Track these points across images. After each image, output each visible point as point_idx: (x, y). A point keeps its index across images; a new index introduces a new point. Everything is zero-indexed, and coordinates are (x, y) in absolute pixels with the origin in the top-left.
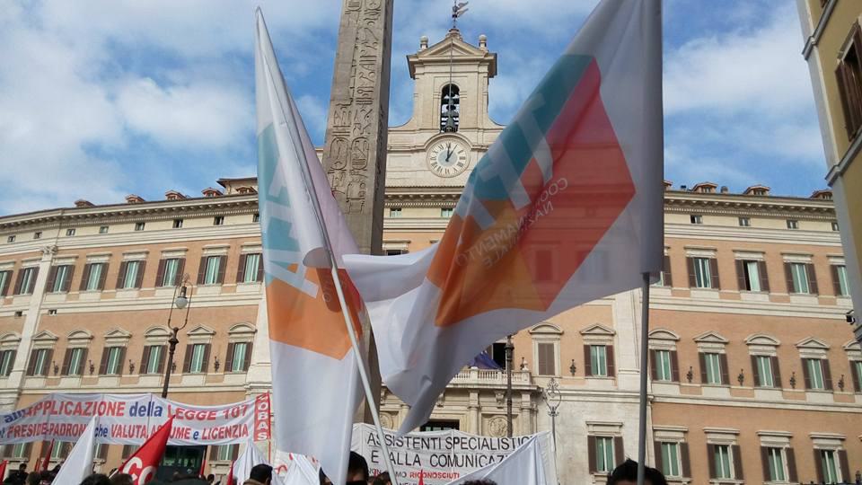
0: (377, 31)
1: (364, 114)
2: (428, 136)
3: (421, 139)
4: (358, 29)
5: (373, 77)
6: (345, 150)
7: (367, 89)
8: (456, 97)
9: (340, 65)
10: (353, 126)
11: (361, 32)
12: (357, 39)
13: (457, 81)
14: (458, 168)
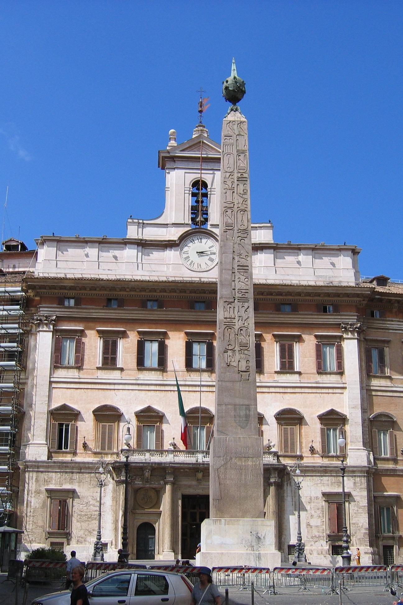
0: (247, 246)
1: (244, 309)
2: (182, 231)
3: (174, 234)
4: (234, 244)
5: (247, 281)
6: (233, 336)
7: (244, 291)
8: (204, 191)
9: (223, 271)
10: (237, 318)
11: (236, 246)
12: (234, 251)
13: (207, 177)
14: (209, 263)
